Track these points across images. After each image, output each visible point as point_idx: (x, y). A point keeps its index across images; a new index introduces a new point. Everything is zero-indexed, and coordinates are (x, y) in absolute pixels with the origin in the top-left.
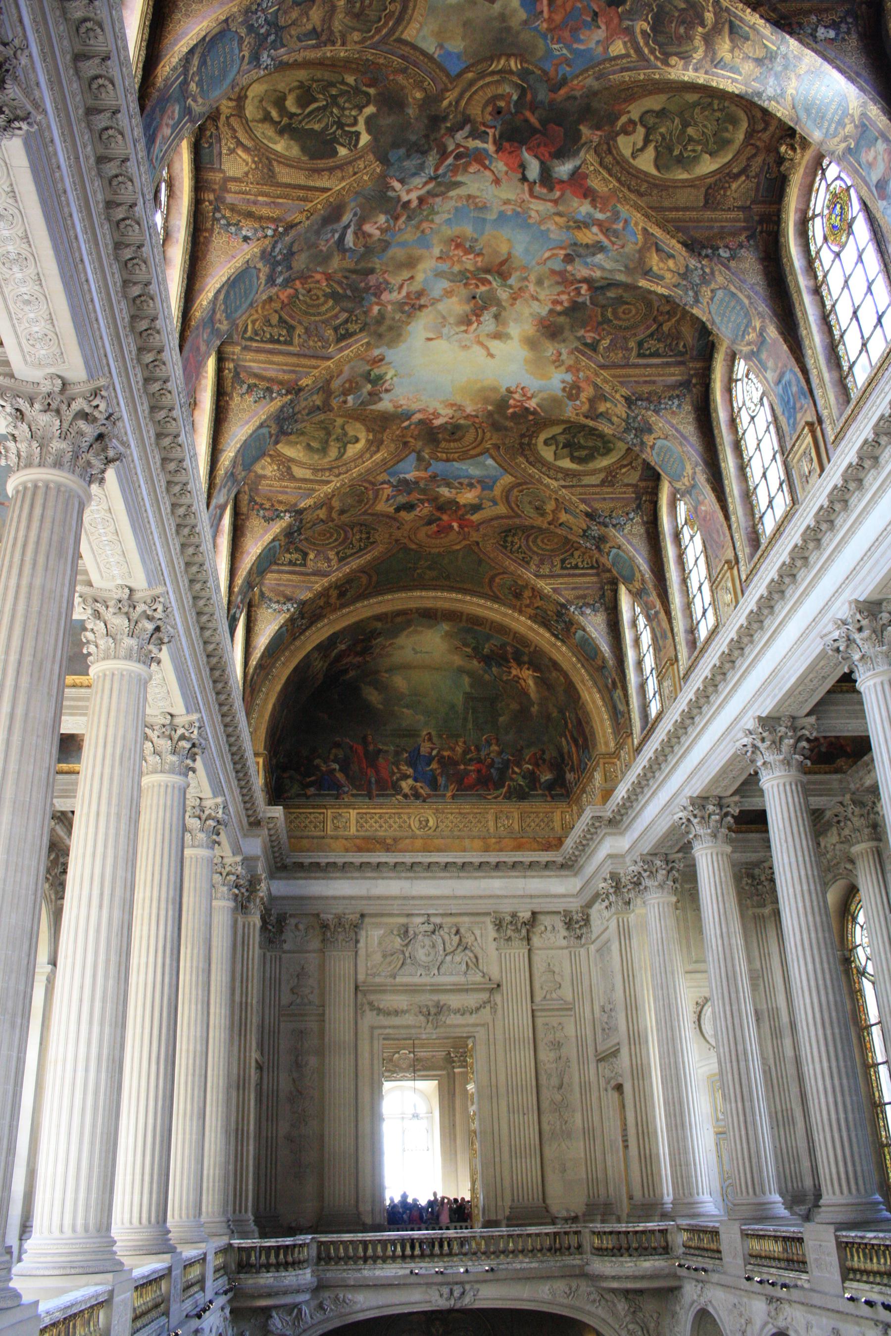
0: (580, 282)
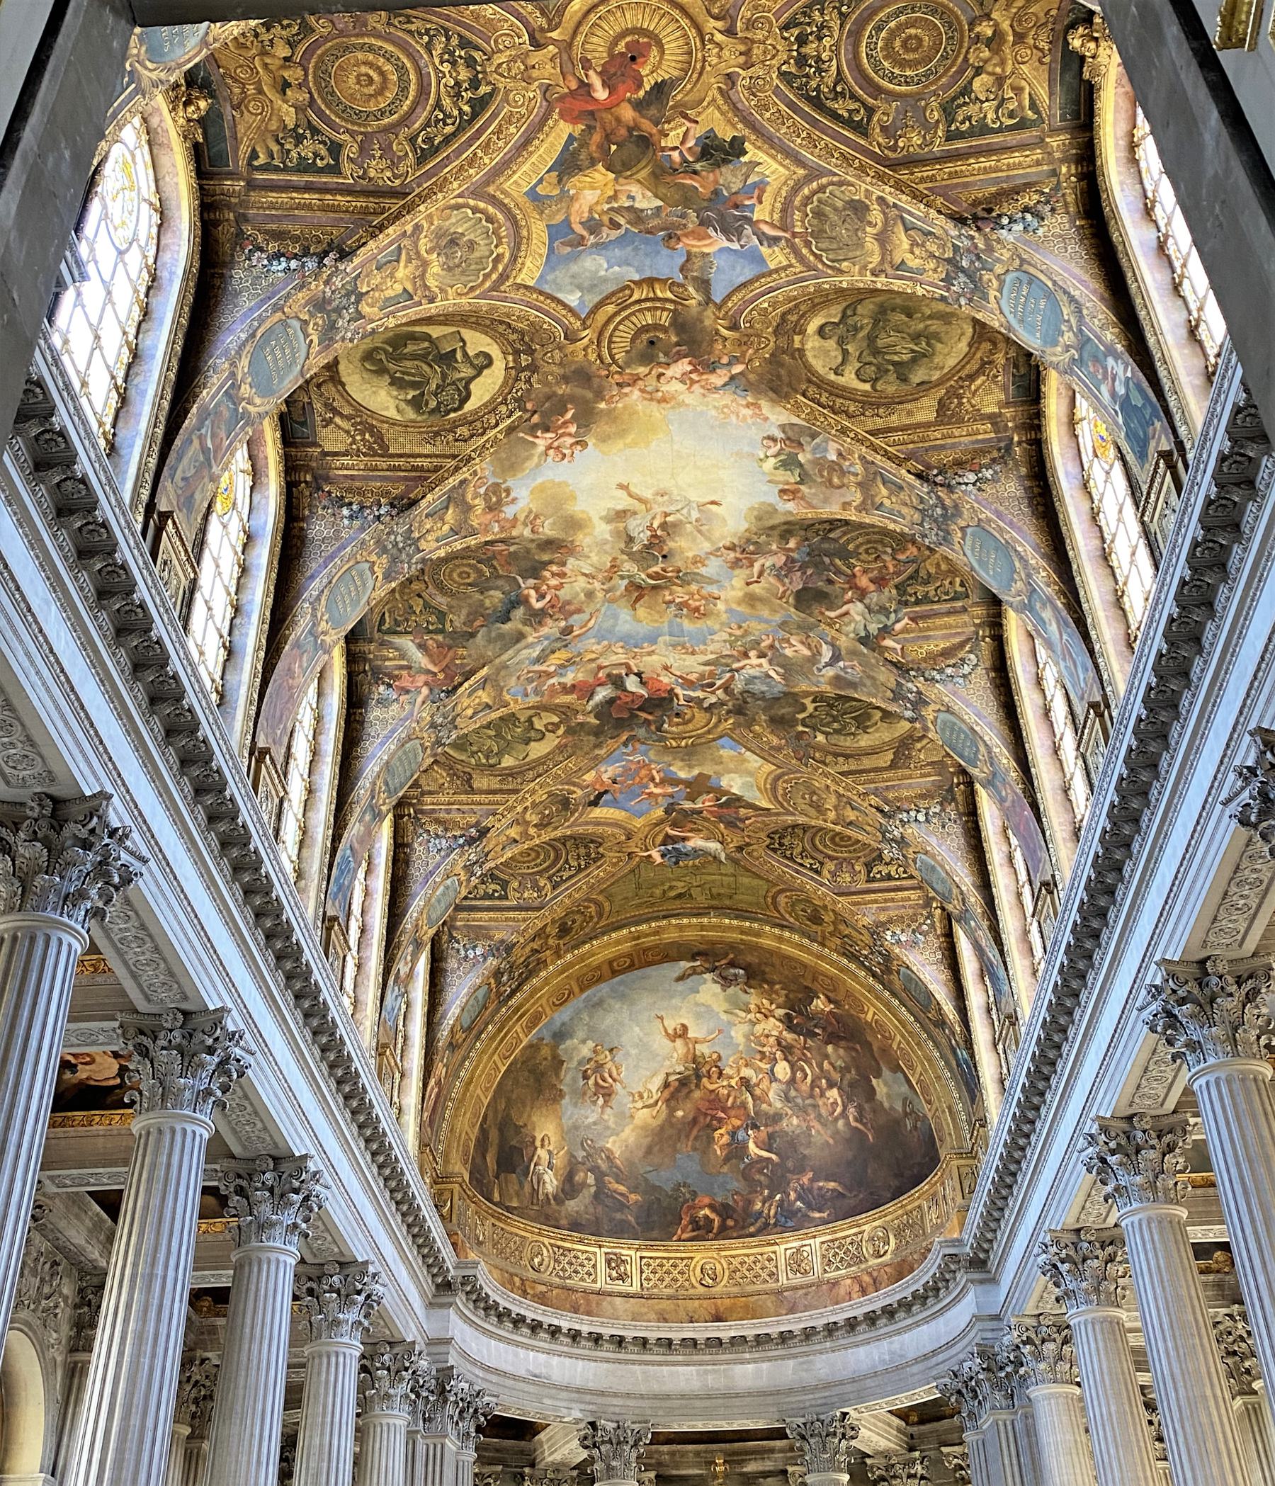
0: (542, 609)
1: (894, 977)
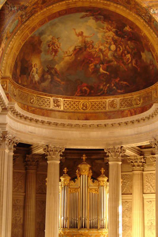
1: (152, 23)
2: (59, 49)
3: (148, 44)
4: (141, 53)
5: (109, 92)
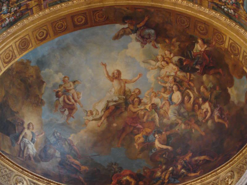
2: (78, 104)
3: (239, 60)
4: (227, 90)
5: (173, 180)
